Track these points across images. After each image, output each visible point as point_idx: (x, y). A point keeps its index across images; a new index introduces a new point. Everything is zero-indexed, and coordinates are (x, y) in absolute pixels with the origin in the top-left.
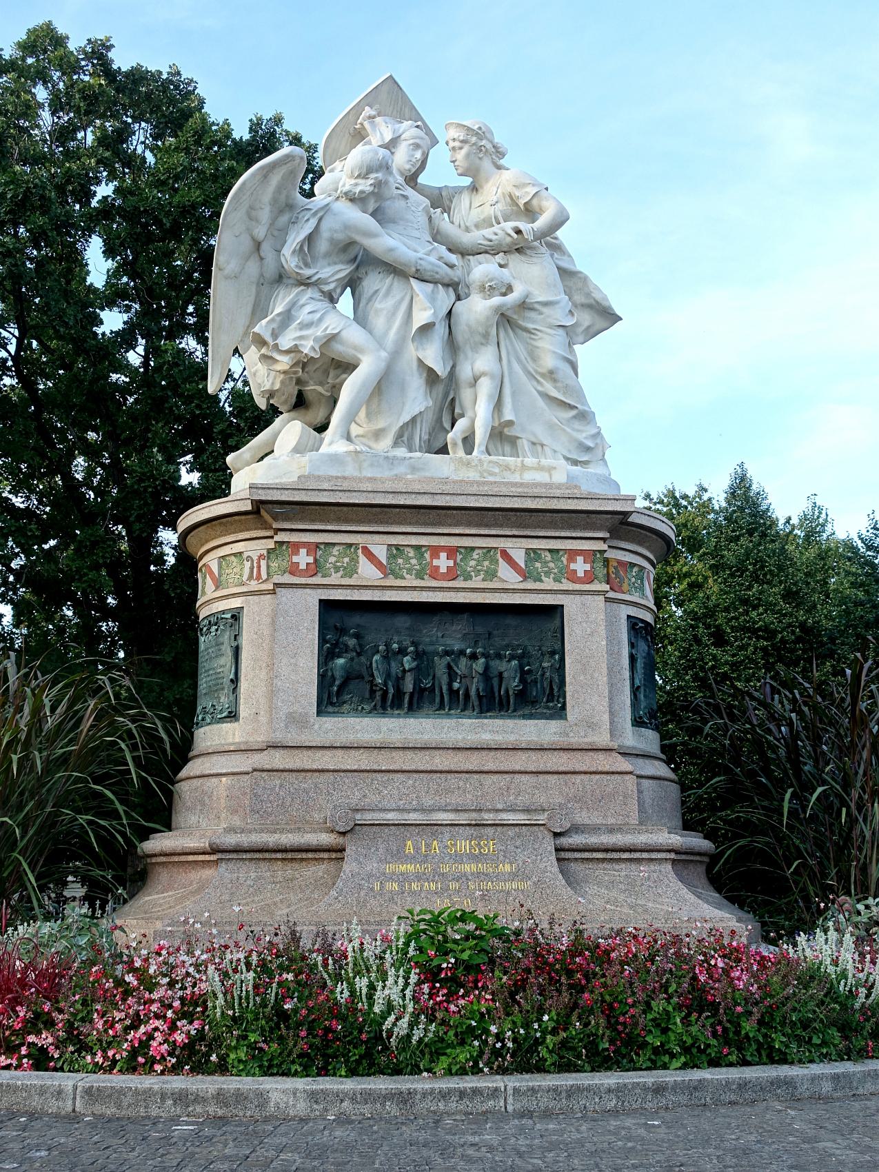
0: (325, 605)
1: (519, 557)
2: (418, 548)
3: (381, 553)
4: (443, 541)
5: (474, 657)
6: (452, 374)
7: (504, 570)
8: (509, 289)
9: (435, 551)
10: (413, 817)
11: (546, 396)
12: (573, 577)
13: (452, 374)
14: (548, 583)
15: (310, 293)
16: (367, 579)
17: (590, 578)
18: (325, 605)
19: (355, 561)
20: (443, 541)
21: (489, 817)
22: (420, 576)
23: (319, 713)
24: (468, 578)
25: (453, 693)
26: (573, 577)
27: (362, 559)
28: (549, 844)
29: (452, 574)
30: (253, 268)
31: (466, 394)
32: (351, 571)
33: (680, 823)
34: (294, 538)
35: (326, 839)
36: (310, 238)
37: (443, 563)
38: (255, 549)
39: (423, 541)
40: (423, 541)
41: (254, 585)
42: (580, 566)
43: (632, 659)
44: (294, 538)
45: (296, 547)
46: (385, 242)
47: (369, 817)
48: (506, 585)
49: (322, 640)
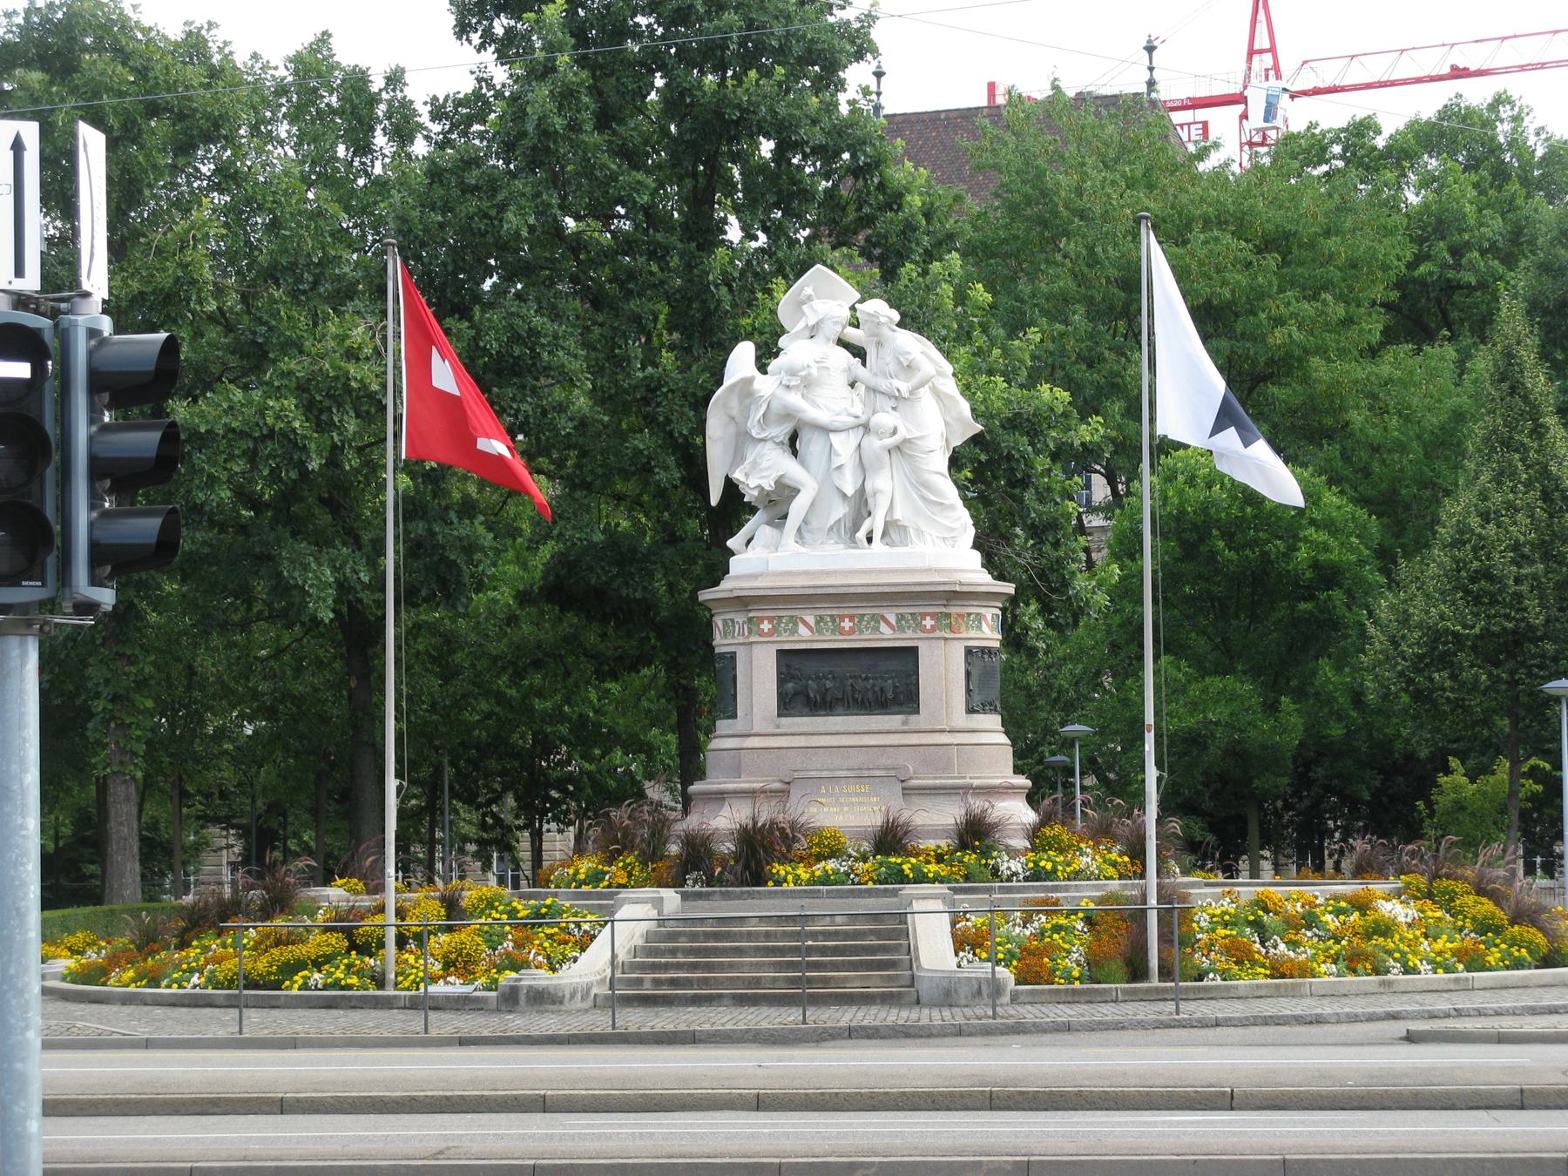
0: (782, 654)
1: (892, 619)
2: (832, 616)
3: (811, 620)
4: (846, 612)
5: (867, 679)
6: (861, 491)
7: (884, 627)
8: (895, 432)
9: (842, 618)
10: (825, 774)
11: (924, 499)
12: (924, 630)
13: (861, 491)
14: (909, 634)
15: (769, 445)
16: (805, 636)
17: (933, 629)
18: (782, 654)
19: (796, 625)
20: (846, 612)
21: (866, 773)
22: (833, 632)
23: (779, 715)
24: (861, 632)
25: (856, 700)
26: (924, 630)
27: (801, 626)
28: (899, 786)
29: (852, 631)
30: (732, 429)
31: (870, 501)
32: (794, 631)
33: (1011, 769)
34: (760, 614)
35: (777, 785)
36: (764, 415)
37: (847, 624)
38: (740, 618)
39: (835, 612)
40: (835, 612)
41: (741, 639)
42: (928, 623)
43: (968, 674)
44: (760, 614)
45: (761, 620)
46: (813, 413)
47: (801, 774)
48: (886, 636)
49: (779, 673)
